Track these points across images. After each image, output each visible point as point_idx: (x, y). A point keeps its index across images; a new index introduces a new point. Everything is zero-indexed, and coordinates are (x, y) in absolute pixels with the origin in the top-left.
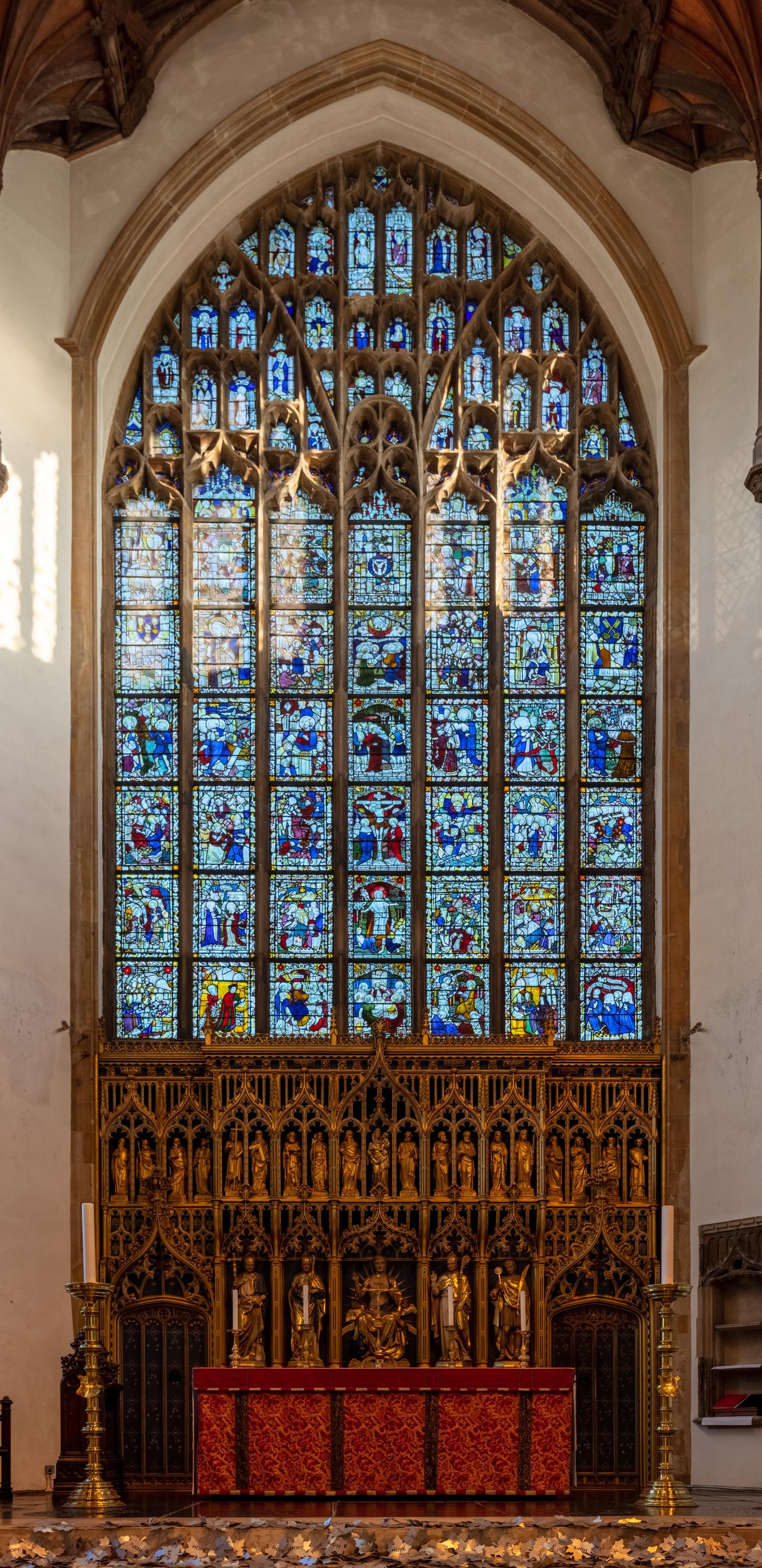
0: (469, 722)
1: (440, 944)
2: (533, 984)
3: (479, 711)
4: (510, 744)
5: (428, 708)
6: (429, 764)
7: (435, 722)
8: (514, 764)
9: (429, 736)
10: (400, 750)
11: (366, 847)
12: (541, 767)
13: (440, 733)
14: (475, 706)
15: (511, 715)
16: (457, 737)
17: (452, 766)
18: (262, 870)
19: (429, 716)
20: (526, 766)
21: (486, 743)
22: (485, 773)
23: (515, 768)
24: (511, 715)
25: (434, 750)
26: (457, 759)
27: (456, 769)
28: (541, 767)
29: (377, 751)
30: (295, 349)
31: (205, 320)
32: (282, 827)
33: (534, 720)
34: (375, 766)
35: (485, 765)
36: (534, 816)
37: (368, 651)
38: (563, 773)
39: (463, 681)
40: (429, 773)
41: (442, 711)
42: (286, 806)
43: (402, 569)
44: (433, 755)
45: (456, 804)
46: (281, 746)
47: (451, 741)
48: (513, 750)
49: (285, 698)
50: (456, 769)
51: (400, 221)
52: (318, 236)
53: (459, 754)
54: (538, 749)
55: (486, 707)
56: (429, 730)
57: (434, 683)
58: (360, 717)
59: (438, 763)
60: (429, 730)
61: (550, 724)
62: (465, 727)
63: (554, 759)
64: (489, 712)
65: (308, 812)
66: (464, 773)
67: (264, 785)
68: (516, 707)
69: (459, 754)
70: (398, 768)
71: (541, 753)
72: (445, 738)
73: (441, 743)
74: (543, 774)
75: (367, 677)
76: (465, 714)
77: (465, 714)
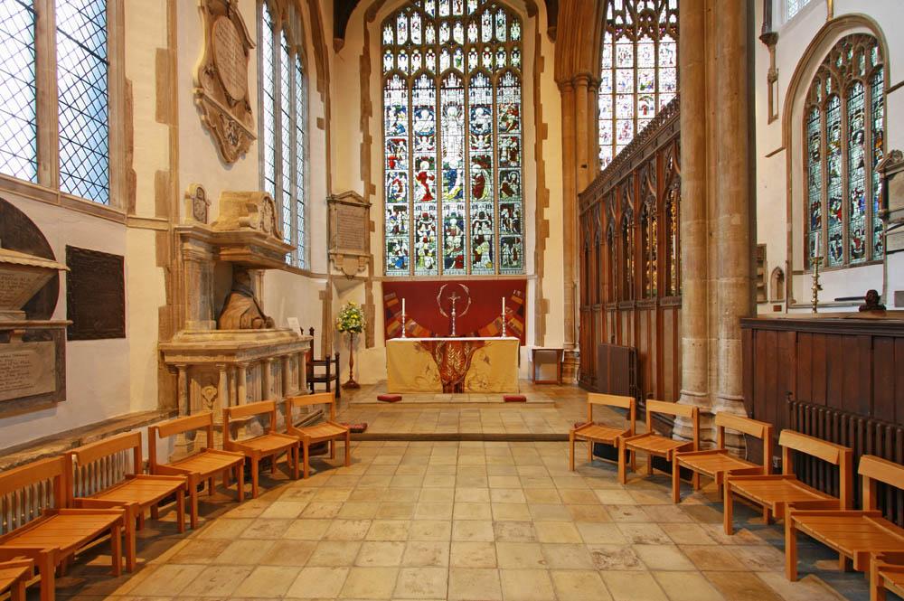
10: (652, 109)
29: (646, 109)
32: (619, 133)
34: (645, 113)
37: (643, 81)
39: (669, 88)
43: (653, 57)
49: (621, 94)
57: (660, 90)
58: (641, 99)
65: (626, 127)
67: (614, 120)
75: (643, 88)
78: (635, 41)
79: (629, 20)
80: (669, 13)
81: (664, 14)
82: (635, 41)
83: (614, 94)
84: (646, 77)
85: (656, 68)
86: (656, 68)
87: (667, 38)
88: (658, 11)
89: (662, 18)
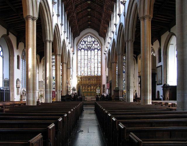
1: (92, 71)
2: (96, 73)
11: (89, 66)
18: (84, 68)
30: (86, 44)
31: (82, 42)
32: (85, 66)
36: (96, 65)
42: (85, 65)
45: (93, 64)
46: (85, 62)
51: (90, 38)
52: (87, 39)
70: (90, 63)
78: (88, 51)
79: (87, 48)
80: (93, 47)
81: (92, 47)
82: (88, 51)
83: (84, 60)
84: (89, 57)
85: (91, 56)
86: (91, 56)
87: (93, 51)
88: (91, 47)
89: (92, 48)
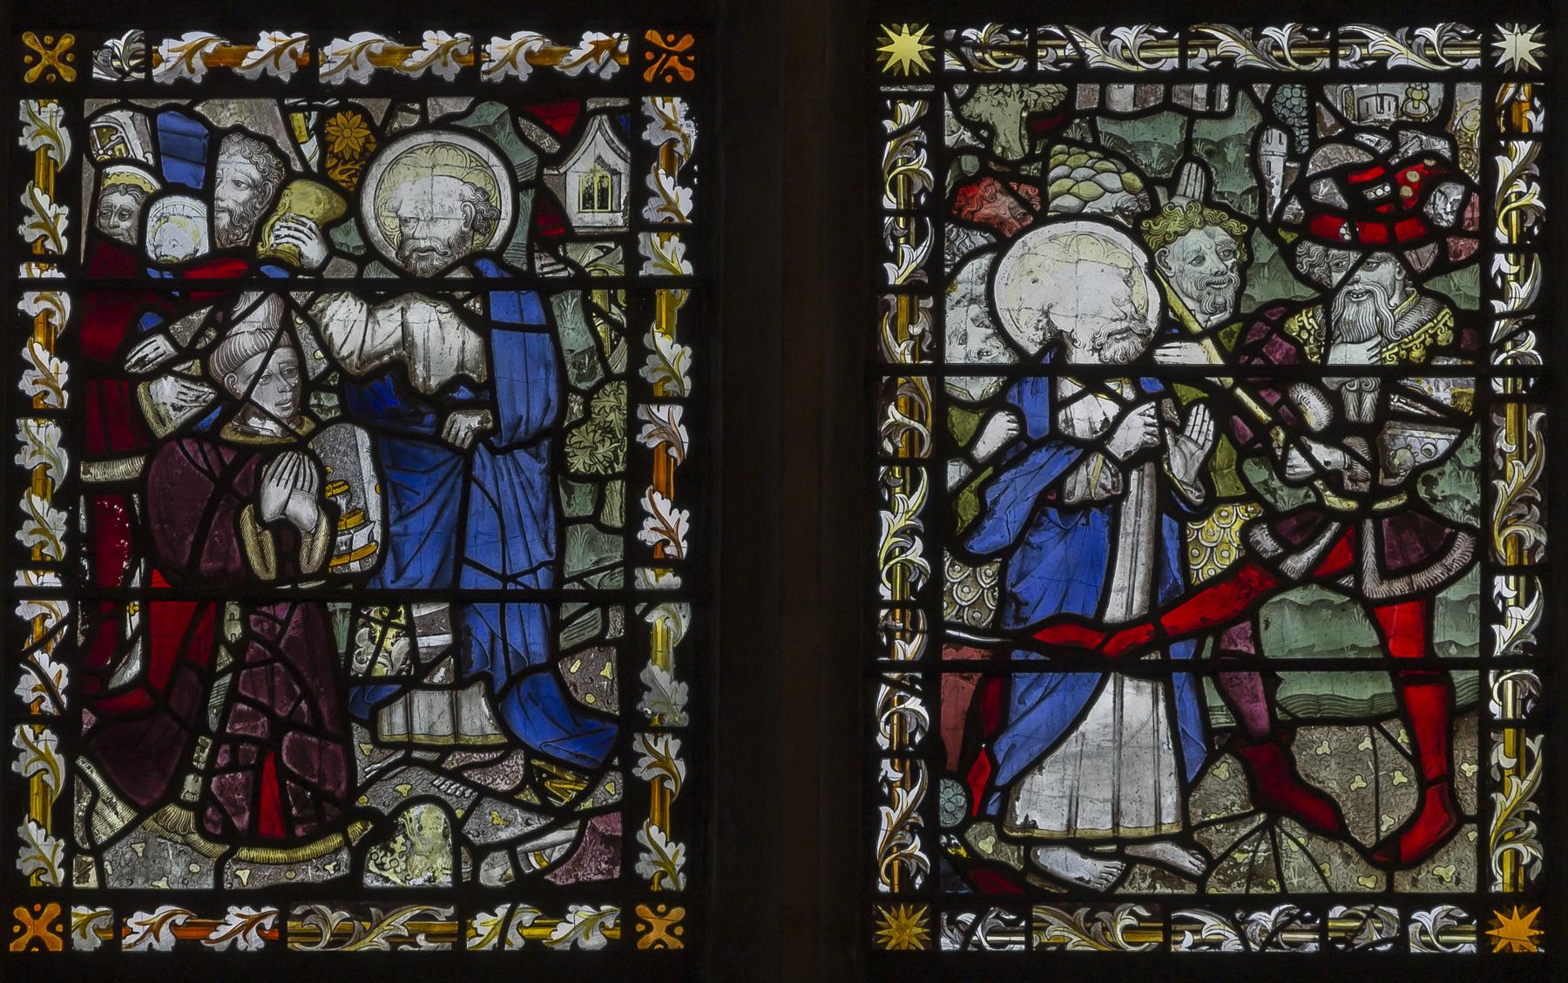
0: (467, 282)
3: (594, 160)
4: (942, 529)
5: (43, 127)
6: (38, 753)
7: (119, 289)
8: (974, 758)
9: (42, 443)
12: (1282, 793)
13: (169, 398)
14: (553, 106)
15: (939, 210)
16: (355, 452)
17: (303, 783)
19: (45, 215)
20: (1104, 768)
21: (666, 521)
22: (663, 851)
23: (991, 795)
24: (939, 210)
25: (94, 595)
26: (355, 700)
27: (332, 806)
28: (1282, 793)
33: (1202, 251)
35: (662, 759)
38: (1519, 855)
40: (40, 848)
41: (188, 166)
44: (89, 656)
47: (285, 495)
48: (968, 592)
50: (332, 806)
53: (382, 650)
54: (1254, 581)
55: (671, 116)
56: (46, 370)
59: (131, 741)
60: (46, 370)
61: (1377, 308)
62: (439, 337)
63: (1425, 696)
64: (700, 169)
66: (421, 856)
68: (1005, 114)
69: (382, 650)
71: (1287, 627)
72: (223, 463)
73: (170, 528)
74: (1303, 861)
76: (432, 194)
77: (432, 194)
